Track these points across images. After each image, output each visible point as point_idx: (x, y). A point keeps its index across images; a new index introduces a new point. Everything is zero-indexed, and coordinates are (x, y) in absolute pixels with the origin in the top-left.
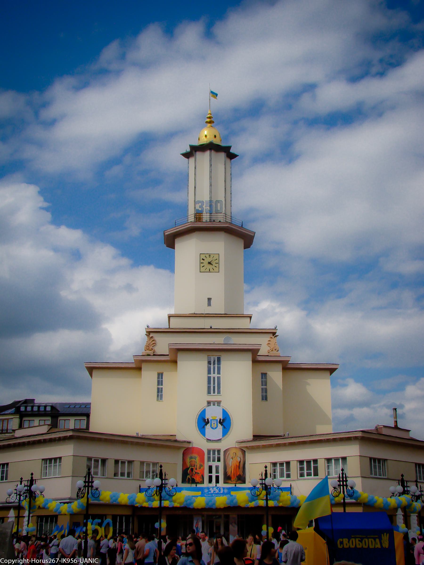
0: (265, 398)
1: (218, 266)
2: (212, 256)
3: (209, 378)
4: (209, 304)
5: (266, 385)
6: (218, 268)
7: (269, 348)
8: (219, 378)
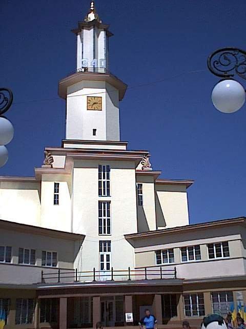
3: (100, 183)
4: (94, 134)
8: (108, 182)
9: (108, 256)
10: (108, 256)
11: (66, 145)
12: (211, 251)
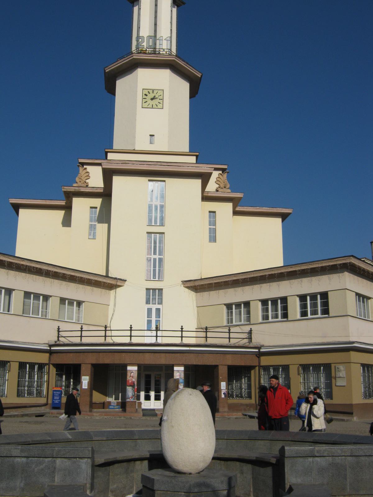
0: (213, 238)
1: (162, 103)
2: (155, 92)
5: (215, 224)
6: (161, 105)
7: (218, 186)
9: (158, 310)
10: (158, 310)
11: (110, 156)
12: (304, 306)
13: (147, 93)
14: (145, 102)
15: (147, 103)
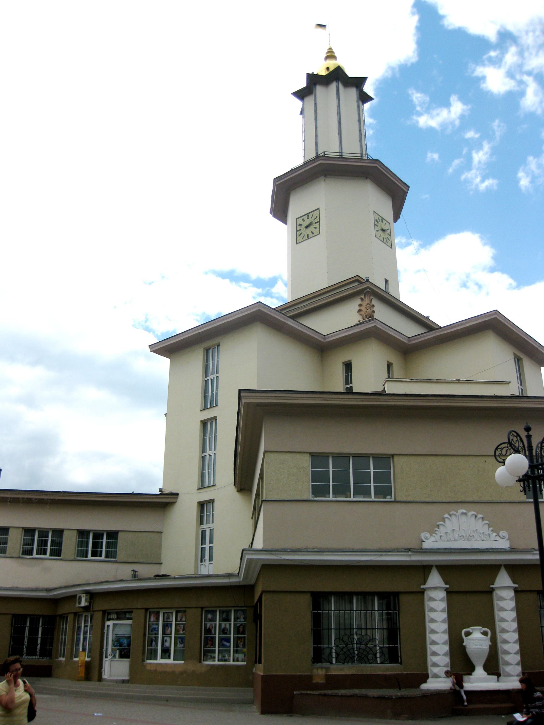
13: (302, 222)
14: (299, 235)
15: (302, 236)
